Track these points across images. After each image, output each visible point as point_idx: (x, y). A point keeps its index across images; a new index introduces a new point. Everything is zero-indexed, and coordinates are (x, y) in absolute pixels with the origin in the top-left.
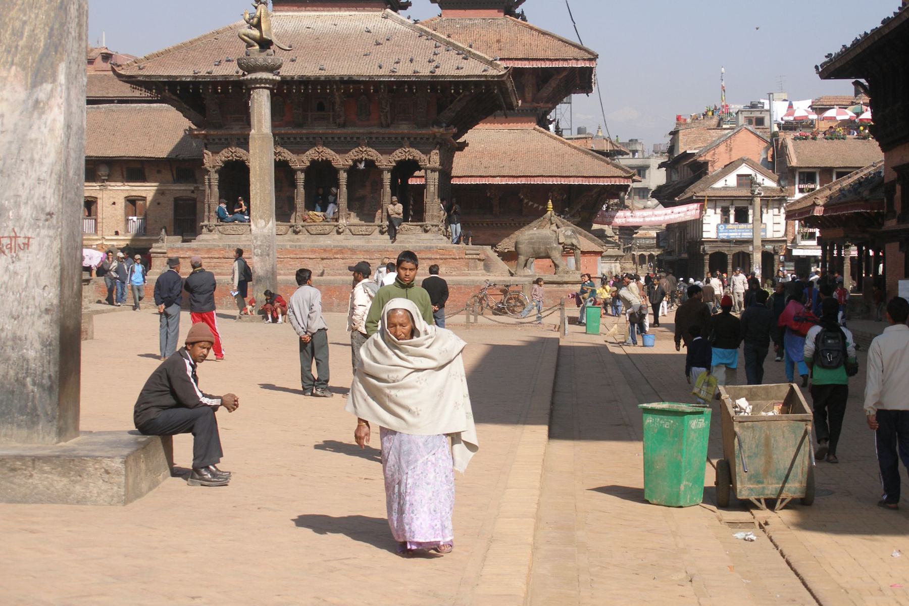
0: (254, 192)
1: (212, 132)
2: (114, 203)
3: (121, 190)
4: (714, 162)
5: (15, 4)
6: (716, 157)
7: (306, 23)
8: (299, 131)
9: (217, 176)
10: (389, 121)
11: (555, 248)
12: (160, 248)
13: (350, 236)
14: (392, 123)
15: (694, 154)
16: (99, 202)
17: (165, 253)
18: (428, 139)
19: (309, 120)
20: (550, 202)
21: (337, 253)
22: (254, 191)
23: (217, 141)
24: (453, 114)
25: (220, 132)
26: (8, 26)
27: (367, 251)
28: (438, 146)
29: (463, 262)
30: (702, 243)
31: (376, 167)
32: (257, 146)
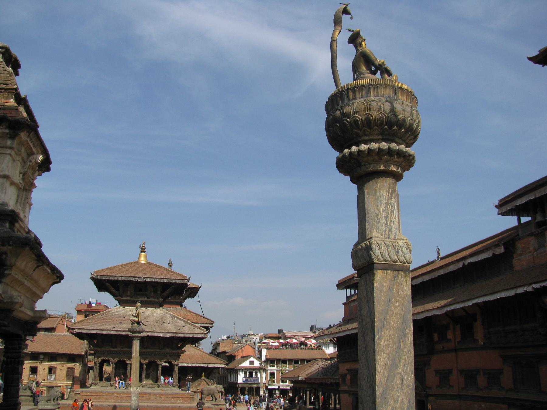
2: (44, 369)
5: (395, 388)
9: (98, 365)
11: (216, 393)
12: (78, 391)
13: (146, 388)
15: (228, 352)
16: (39, 369)
17: (79, 393)
18: (176, 354)
21: (143, 395)
26: (392, 398)
27: (155, 394)
30: (238, 384)
31: (157, 363)
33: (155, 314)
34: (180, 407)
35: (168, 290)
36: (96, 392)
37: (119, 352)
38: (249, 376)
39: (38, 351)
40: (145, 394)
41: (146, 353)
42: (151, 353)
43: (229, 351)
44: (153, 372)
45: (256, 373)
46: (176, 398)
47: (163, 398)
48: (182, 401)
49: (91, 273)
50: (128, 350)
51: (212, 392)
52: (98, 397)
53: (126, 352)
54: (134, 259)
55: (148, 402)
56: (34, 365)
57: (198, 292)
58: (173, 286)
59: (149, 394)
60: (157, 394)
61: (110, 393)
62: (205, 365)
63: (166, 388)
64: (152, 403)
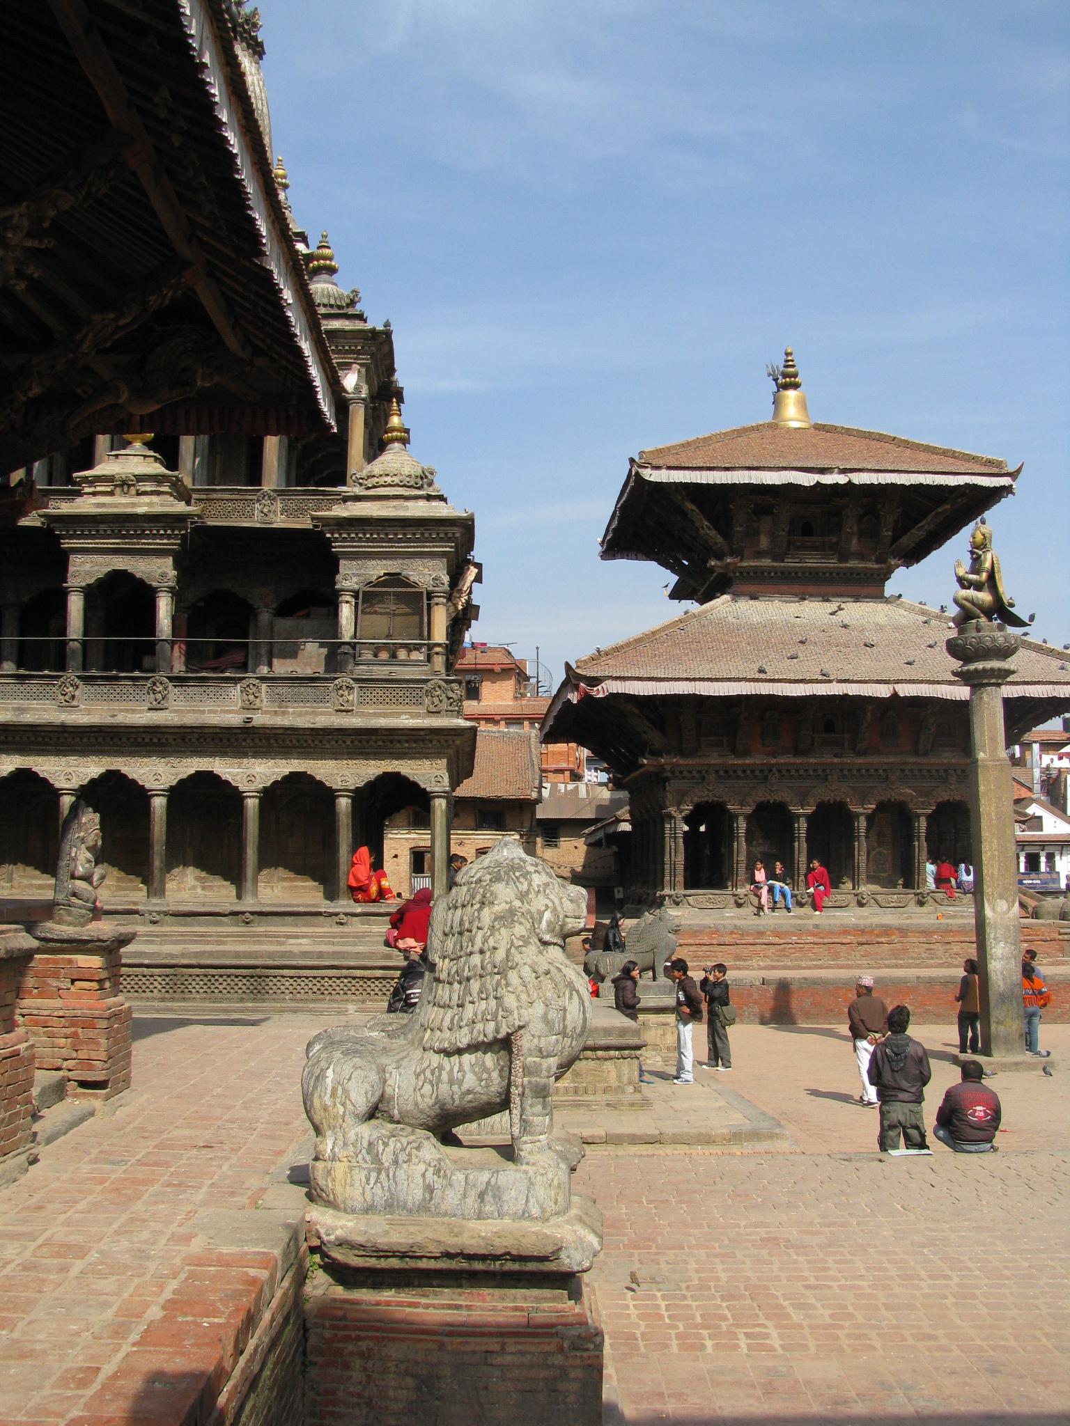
0: (989, 854)
2: (396, 856)
3: (406, 839)
21: (879, 936)
22: (989, 854)
23: (685, 773)
25: (690, 761)
27: (923, 932)
29: (1055, 945)
35: (923, 523)
37: (761, 771)
38: (1026, 869)
40: (887, 930)
44: (879, 846)
45: (1050, 858)
52: (704, 948)
54: (764, 415)
58: (947, 507)
59: (903, 931)
60: (934, 932)
61: (748, 934)
63: (951, 908)
64: (917, 966)
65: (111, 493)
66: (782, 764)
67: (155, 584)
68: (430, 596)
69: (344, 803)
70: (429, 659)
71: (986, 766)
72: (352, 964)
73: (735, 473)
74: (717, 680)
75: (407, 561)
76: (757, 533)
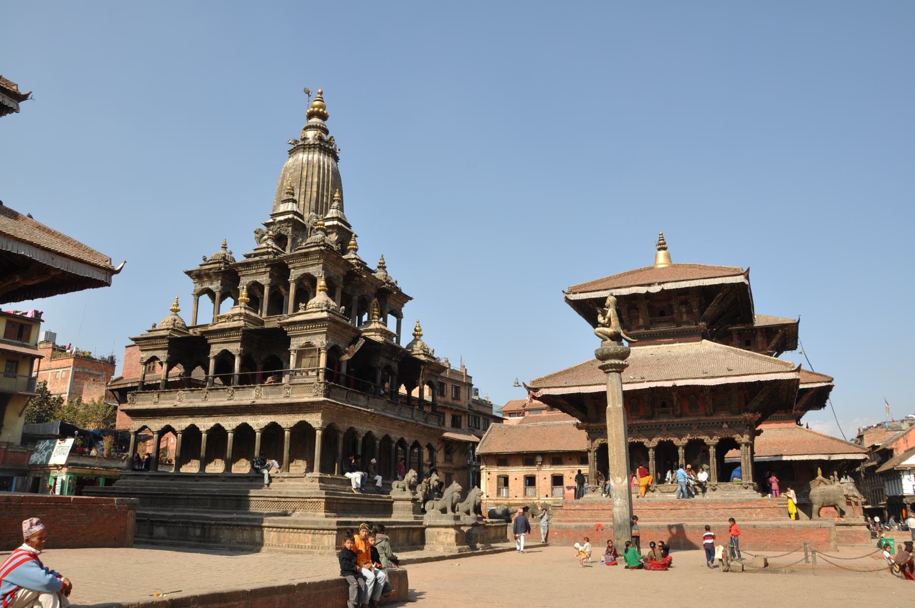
0: (612, 454)
1: (591, 425)
4: (897, 449)
6: (898, 446)
7: (651, 352)
8: (649, 421)
10: (712, 411)
11: (841, 499)
14: (714, 413)
15: (879, 446)
16: (537, 478)
18: (740, 422)
19: (656, 414)
20: (819, 469)
21: (680, 505)
22: (612, 454)
24: (758, 404)
27: (703, 503)
28: (748, 427)
32: (613, 417)
33: (692, 352)
34: (754, 526)
35: (712, 303)
36: (591, 504)
39: (531, 450)
41: (682, 425)
42: (691, 424)
43: (880, 444)
46: (749, 510)
47: (721, 512)
48: (761, 516)
49: (564, 292)
50: (646, 422)
51: (832, 499)
52: (595, 511)
53: (643, 427)
55: (691, 519)
56: (530, 473)
57: (799, 336)
58: (721, 294)
62: (825, 458)
63: (728, 492)
65: (225, 322)
66: (639, 424)
67: (234, 354)
68: (319, 350)
69: (287, 433)
70: (318, 374)
71: (610, 411)
72: (267, 495)
73: (600, 292)
74: (590, 385)
75: (313, 337)
76: (638, 318)
